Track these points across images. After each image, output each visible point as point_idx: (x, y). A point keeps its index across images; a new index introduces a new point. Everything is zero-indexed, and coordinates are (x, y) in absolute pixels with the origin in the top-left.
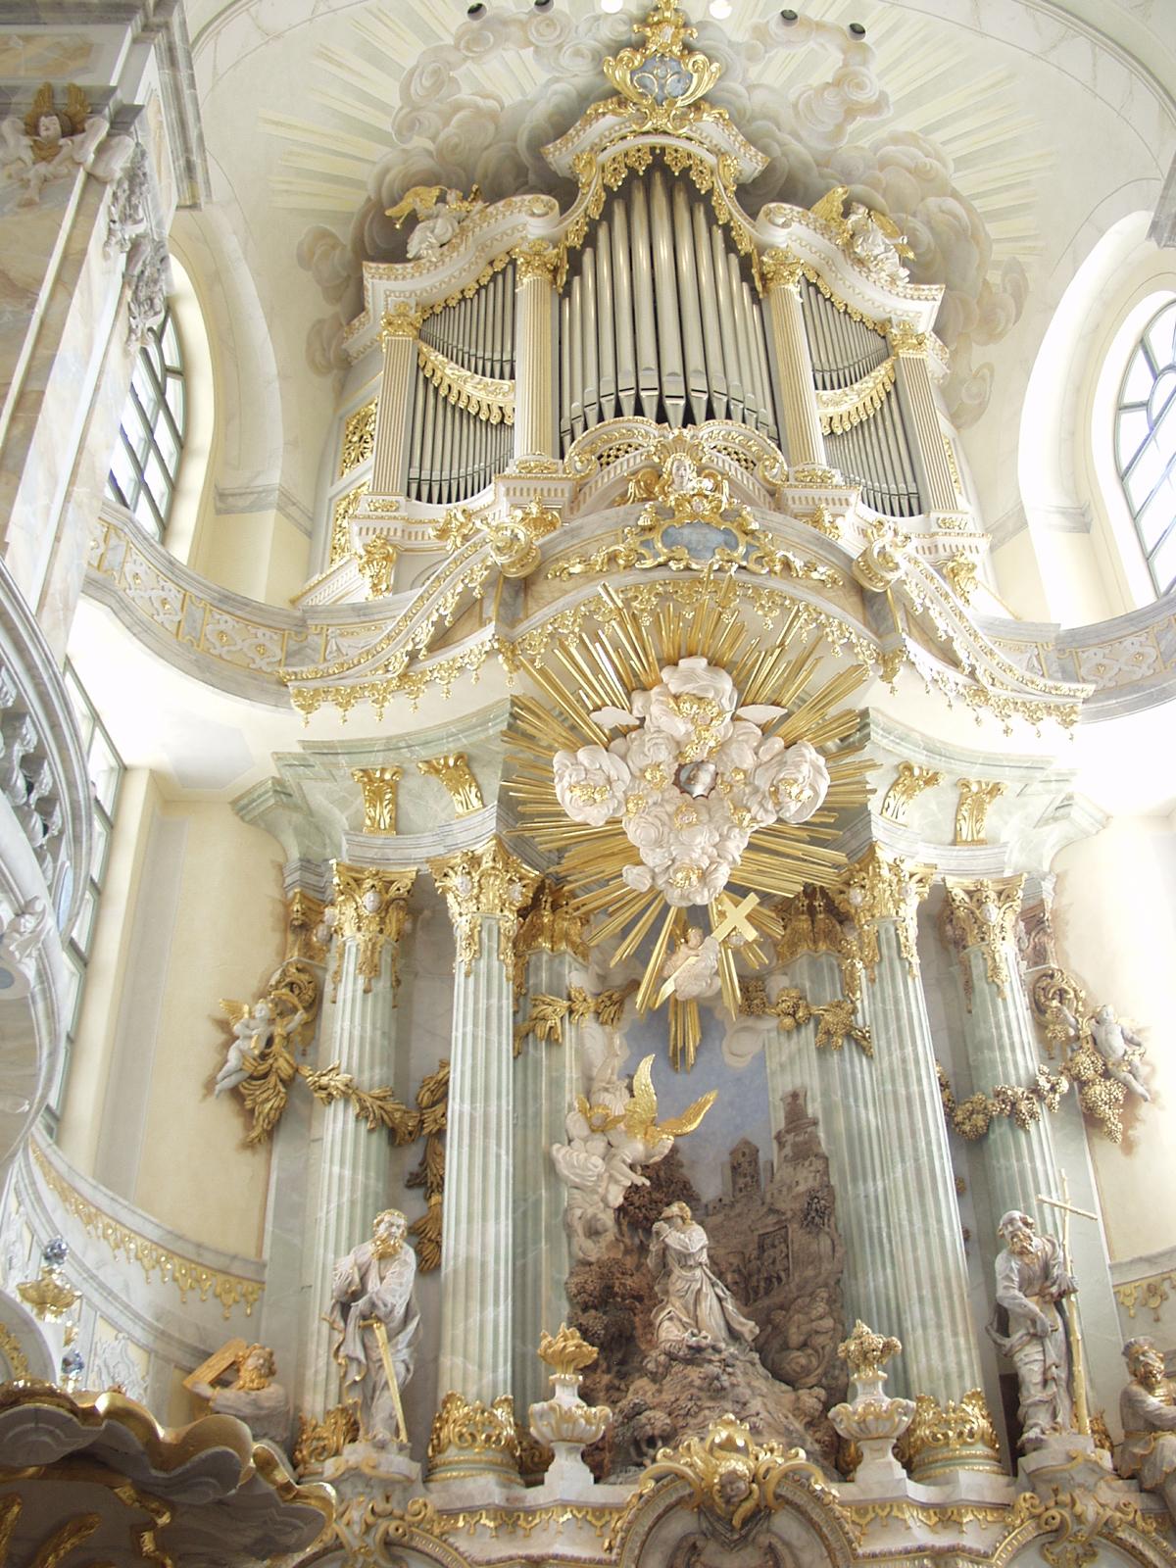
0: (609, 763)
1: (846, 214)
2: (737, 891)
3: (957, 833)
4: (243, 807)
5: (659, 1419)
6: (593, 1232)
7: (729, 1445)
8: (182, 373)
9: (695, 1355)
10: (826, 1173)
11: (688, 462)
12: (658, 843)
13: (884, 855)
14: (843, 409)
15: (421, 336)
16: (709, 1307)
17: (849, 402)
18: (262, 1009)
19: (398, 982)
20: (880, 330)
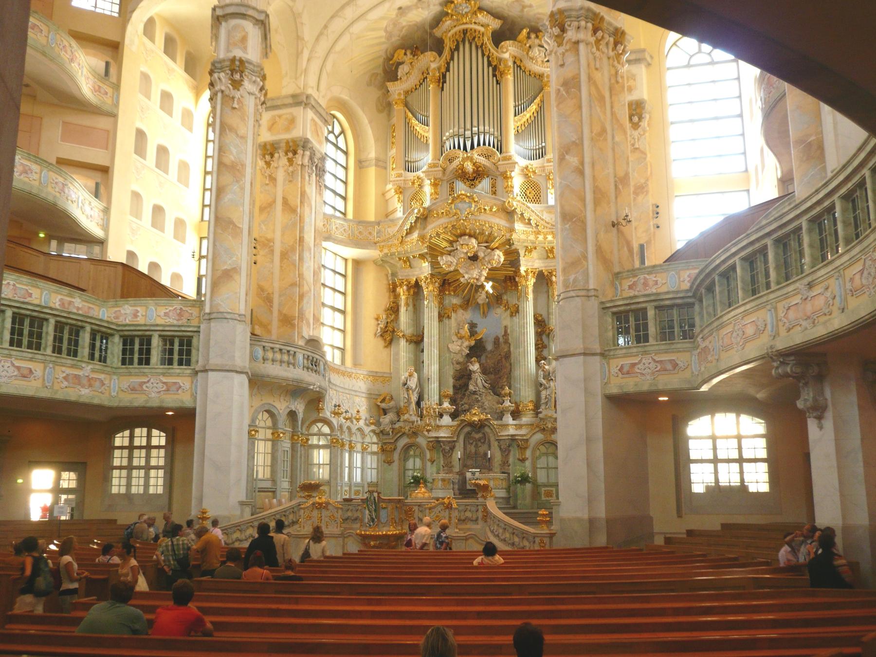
0: (449, 258)
1: (529, 37)
2: (487, 279)
3: (548, 257)
4: (375, 262)
5: (467, 406)
6: (458, 363)
7: (475, 414)
8: (343, 132)
9: (475, 393)
10: (509, 347)
11: (469, 163)
12: (467, 273)
13: (523, 269)
14: (522, 122)
15: (406, 105)
16: (479, 380)
17: (527, 115)
18: (384, 317)
19: (414, 305)
20: (541, 76)
